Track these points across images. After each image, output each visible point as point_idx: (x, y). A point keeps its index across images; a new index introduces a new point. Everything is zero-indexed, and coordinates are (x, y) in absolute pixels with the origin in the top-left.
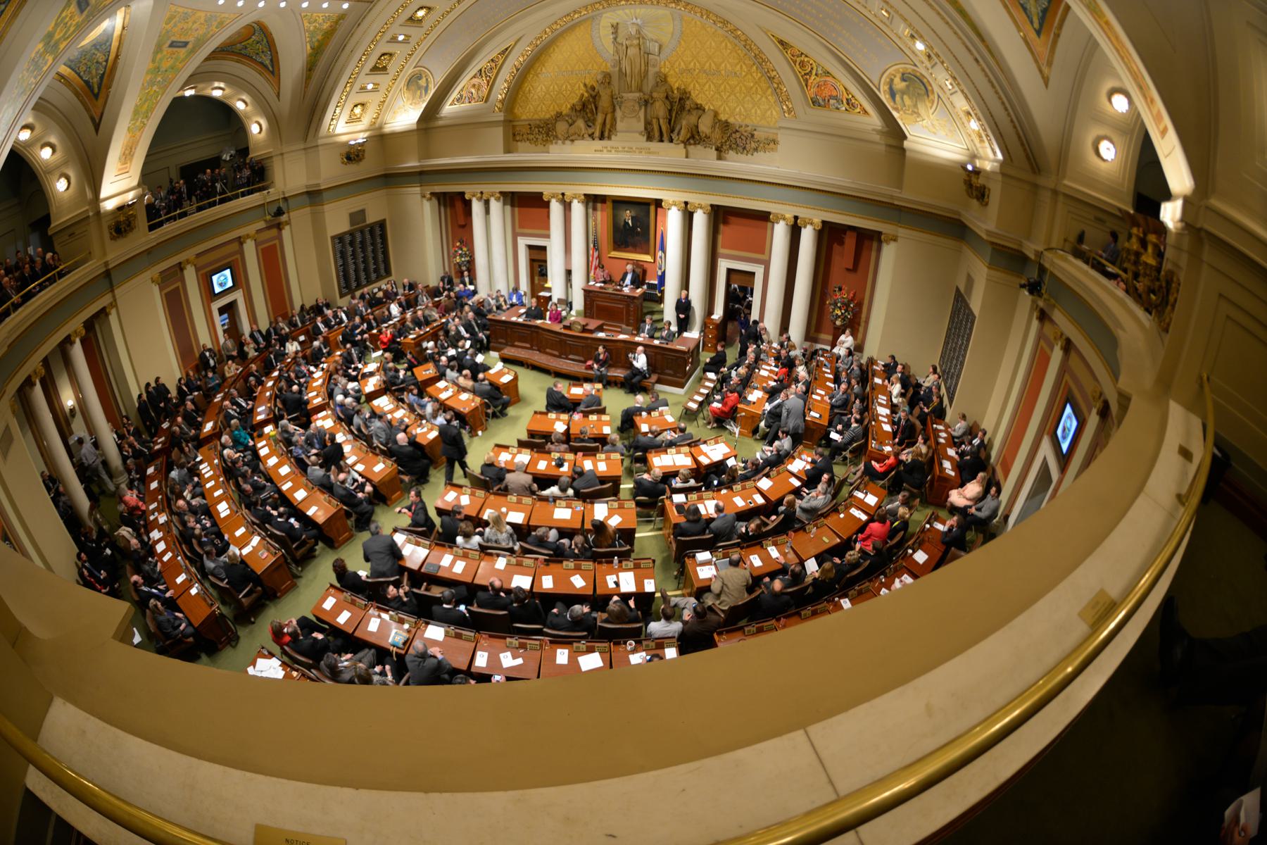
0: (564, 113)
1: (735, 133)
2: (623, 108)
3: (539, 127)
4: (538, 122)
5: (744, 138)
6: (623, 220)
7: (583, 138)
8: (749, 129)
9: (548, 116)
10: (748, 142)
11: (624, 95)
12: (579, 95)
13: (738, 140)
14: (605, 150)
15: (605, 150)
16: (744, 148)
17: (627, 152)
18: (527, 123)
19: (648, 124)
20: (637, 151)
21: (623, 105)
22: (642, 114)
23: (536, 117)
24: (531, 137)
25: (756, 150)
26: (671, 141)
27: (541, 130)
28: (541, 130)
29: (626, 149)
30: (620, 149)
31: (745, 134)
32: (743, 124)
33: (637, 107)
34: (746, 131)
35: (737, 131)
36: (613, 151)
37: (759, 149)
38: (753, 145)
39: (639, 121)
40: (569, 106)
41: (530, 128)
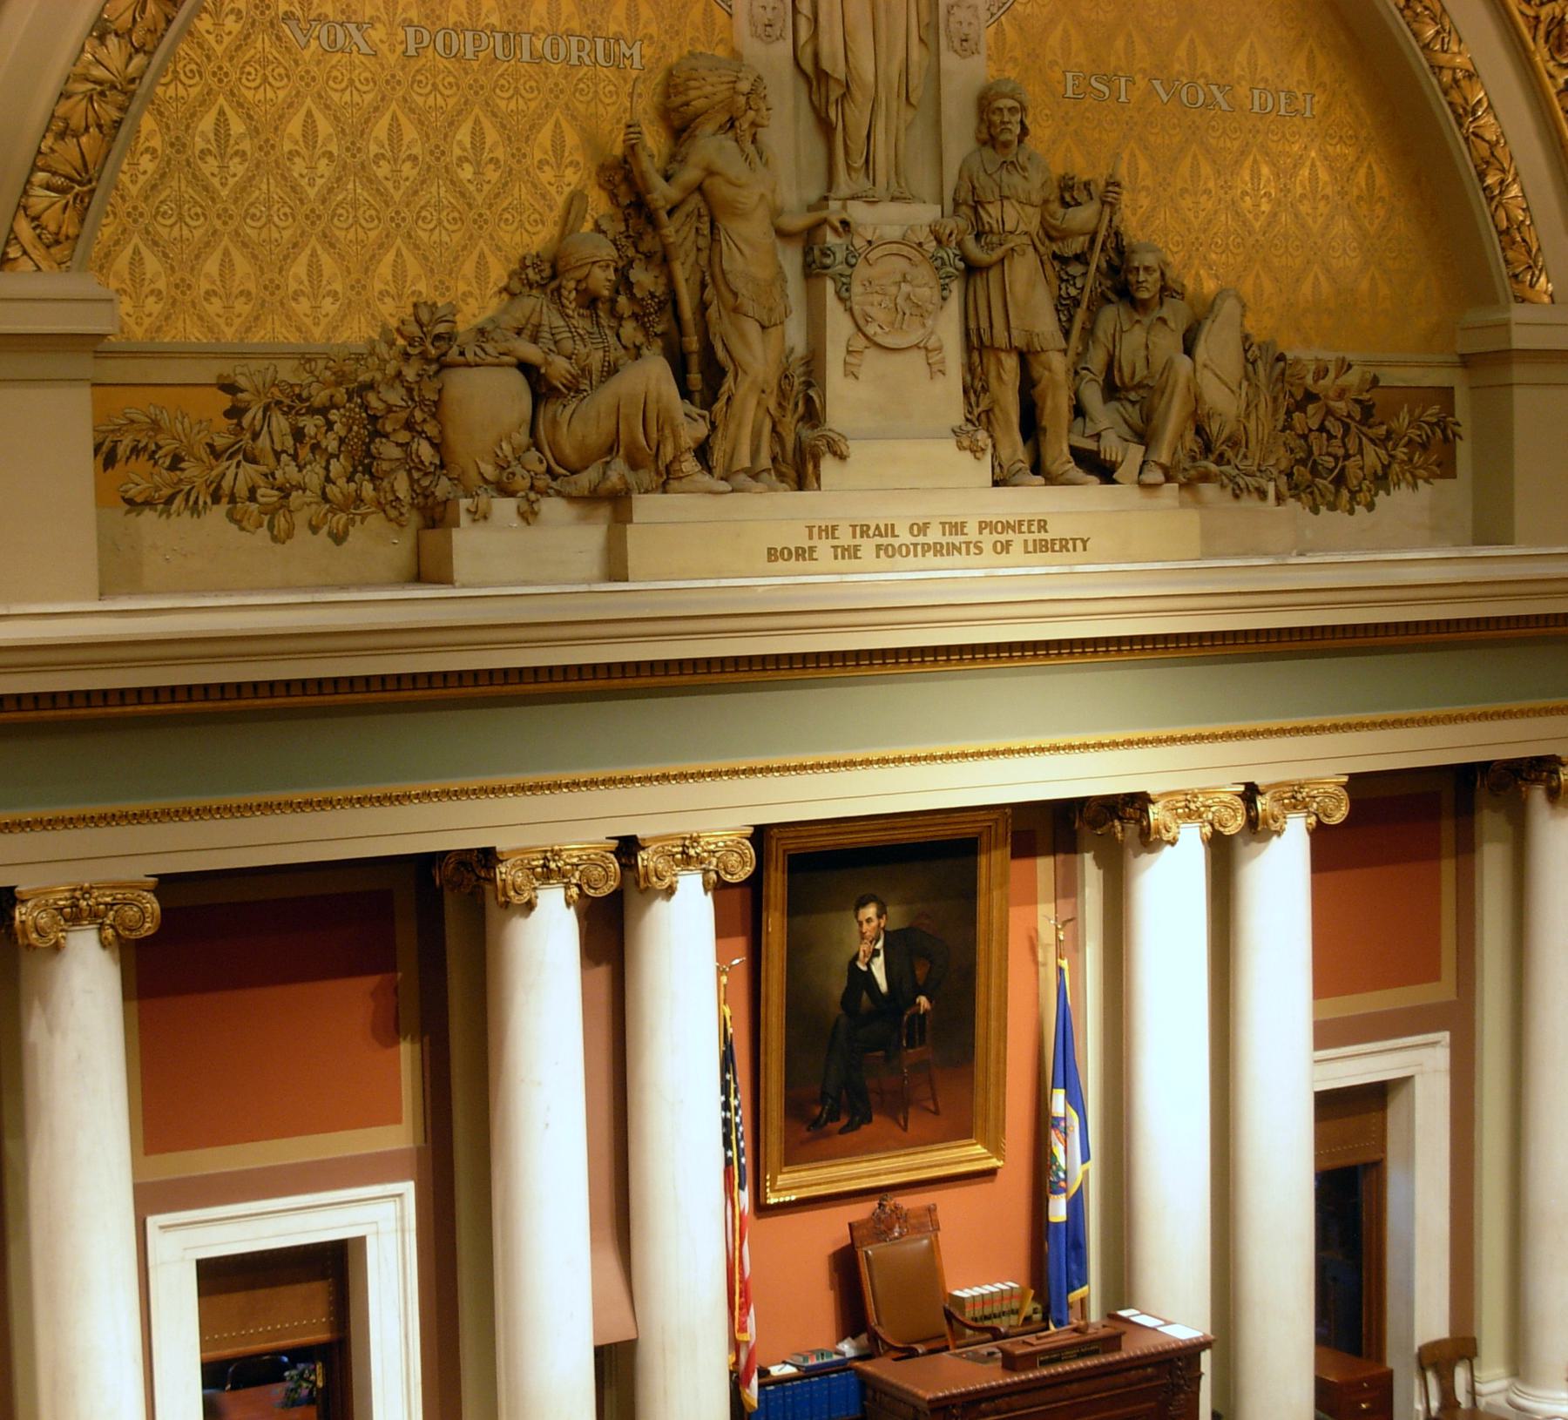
0: (469, 317)
1: (1300, 406)
2: (857, 289)
3: (295, 403)
4: (287, 372)
5: (1337, 430)
6: (842, 960)
7: (667, 480)
8: (1352, 378)
9: (357, 333)
10: (1353, 447)
11: (858, 212)
12: (560, 201)
13: (1318, 442)
14: (824, 547)
15: (824, 547)
16: (1340, 480)
17: (938, 549)
18: (209, 372)
19: (977, 384)
20: (988, 539)
21: (862, 271)
22: (948, 330)
23: (275, 332)
24: (242, 476)
25: (1382, 480)
26: (1105, 472)
27: (311, 425)
28: (311, 425)
29: (934, 535)
30: (905, 537)
31: (1341, 407)
32: (1329, 356)
33: (926, 292)
34: (1341, 395)
35: (1311, 397)
36: (867, 546)
37: (1392, 478)
38: (1373, 457)
39: (936, 370)
40: (498, 273)
41: (235, 412)
